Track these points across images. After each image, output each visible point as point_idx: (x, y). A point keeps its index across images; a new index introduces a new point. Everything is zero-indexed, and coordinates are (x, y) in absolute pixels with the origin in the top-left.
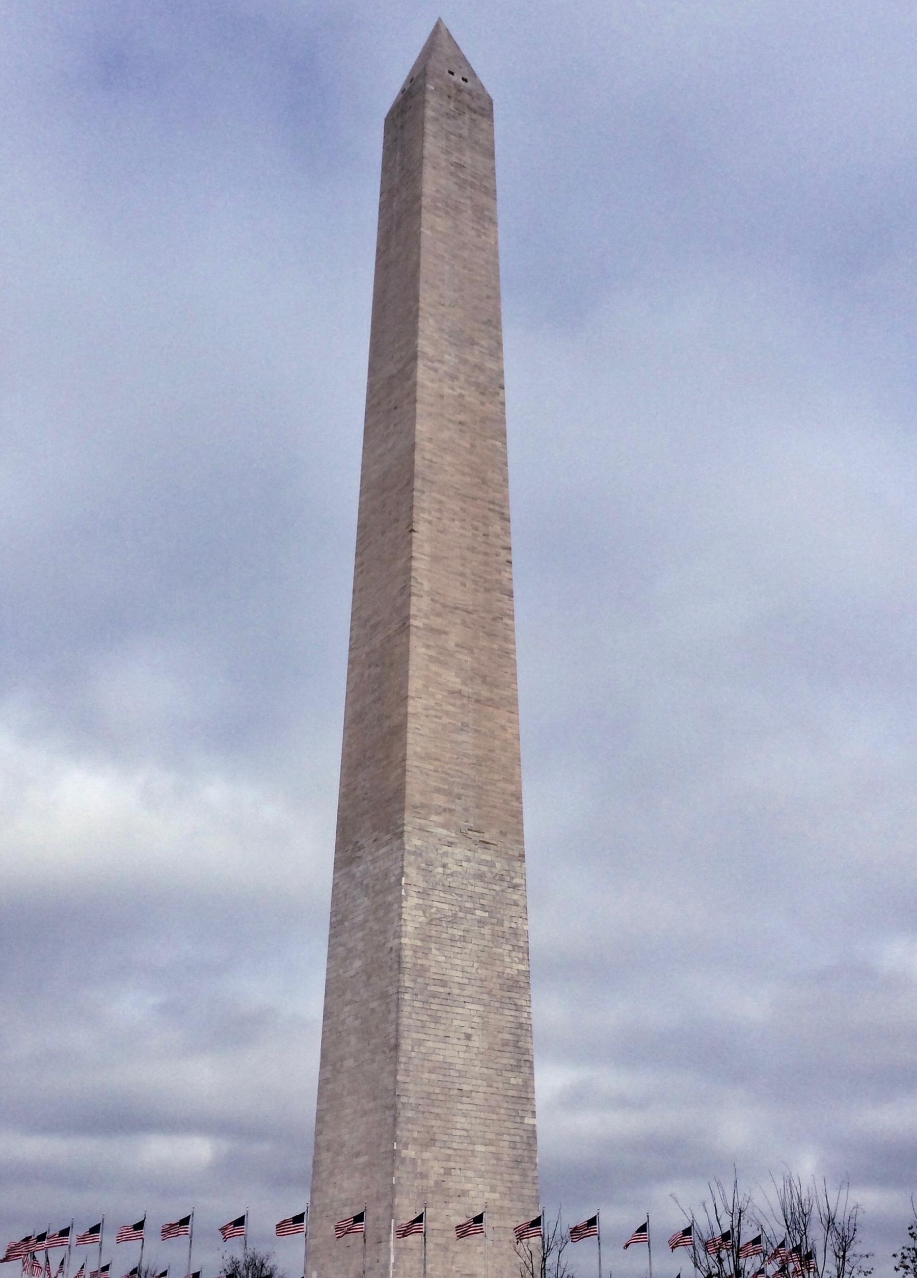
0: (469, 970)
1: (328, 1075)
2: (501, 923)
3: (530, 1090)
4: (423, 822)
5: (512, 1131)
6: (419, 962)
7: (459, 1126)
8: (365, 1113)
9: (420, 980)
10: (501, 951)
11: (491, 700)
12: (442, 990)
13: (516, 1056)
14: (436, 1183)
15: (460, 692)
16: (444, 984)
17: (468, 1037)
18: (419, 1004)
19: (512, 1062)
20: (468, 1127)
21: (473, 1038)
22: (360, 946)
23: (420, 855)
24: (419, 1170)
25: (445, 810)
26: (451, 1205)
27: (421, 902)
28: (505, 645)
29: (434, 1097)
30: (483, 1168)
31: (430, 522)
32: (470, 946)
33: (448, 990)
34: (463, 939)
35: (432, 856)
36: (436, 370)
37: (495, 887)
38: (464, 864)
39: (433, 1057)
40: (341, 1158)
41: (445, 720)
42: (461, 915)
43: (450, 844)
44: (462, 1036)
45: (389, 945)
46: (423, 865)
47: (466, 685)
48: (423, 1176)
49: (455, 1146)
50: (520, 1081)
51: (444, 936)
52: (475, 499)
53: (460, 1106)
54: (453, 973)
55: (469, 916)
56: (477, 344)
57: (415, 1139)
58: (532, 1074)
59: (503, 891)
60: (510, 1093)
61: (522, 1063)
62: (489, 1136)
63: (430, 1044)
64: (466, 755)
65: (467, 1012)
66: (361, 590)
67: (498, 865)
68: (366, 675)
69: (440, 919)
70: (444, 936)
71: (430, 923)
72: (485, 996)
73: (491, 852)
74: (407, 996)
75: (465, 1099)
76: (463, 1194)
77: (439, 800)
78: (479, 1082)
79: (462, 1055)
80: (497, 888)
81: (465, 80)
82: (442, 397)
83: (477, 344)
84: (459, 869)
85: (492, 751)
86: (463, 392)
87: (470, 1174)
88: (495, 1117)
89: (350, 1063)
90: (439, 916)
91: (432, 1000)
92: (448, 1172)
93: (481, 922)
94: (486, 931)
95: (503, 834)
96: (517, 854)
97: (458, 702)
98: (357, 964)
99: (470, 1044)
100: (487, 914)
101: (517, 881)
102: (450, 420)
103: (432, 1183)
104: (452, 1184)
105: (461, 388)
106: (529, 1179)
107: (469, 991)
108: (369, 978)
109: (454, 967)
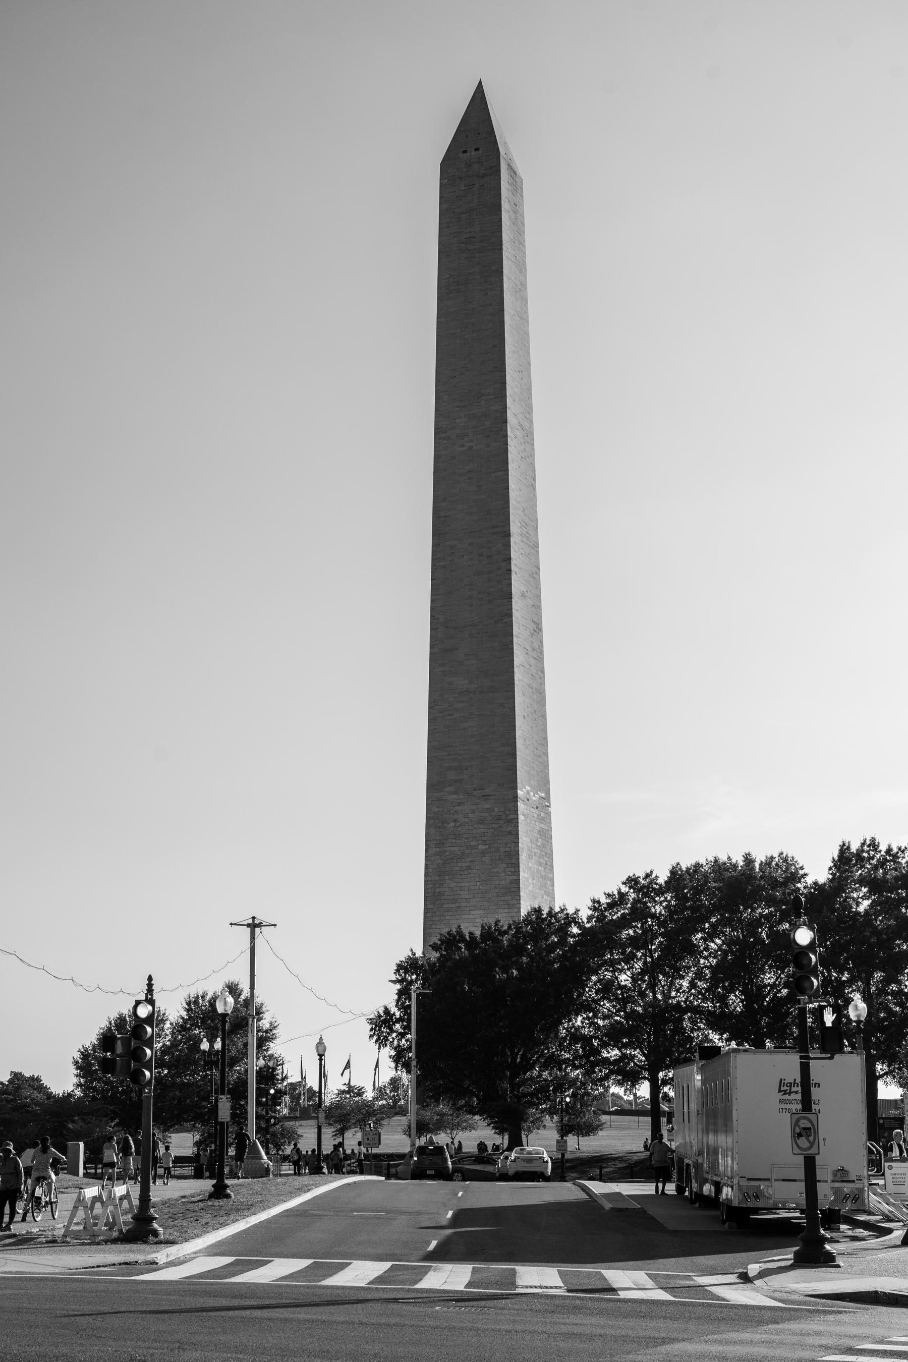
12: (453, 906)
16: (455, 901)
25: (456, 781)
27: (438, 850)
33: (457, 905)
34: (469, 868)
43: (459, 804)
55: (473, 851)
65: (471, 916)
67: (496, 810)
69: (452, 859)
80: (496, 826)
81: (477, 149)
82: (454, 458)
86: (471, 444)
93: (483, 853)
94: (487, 858)
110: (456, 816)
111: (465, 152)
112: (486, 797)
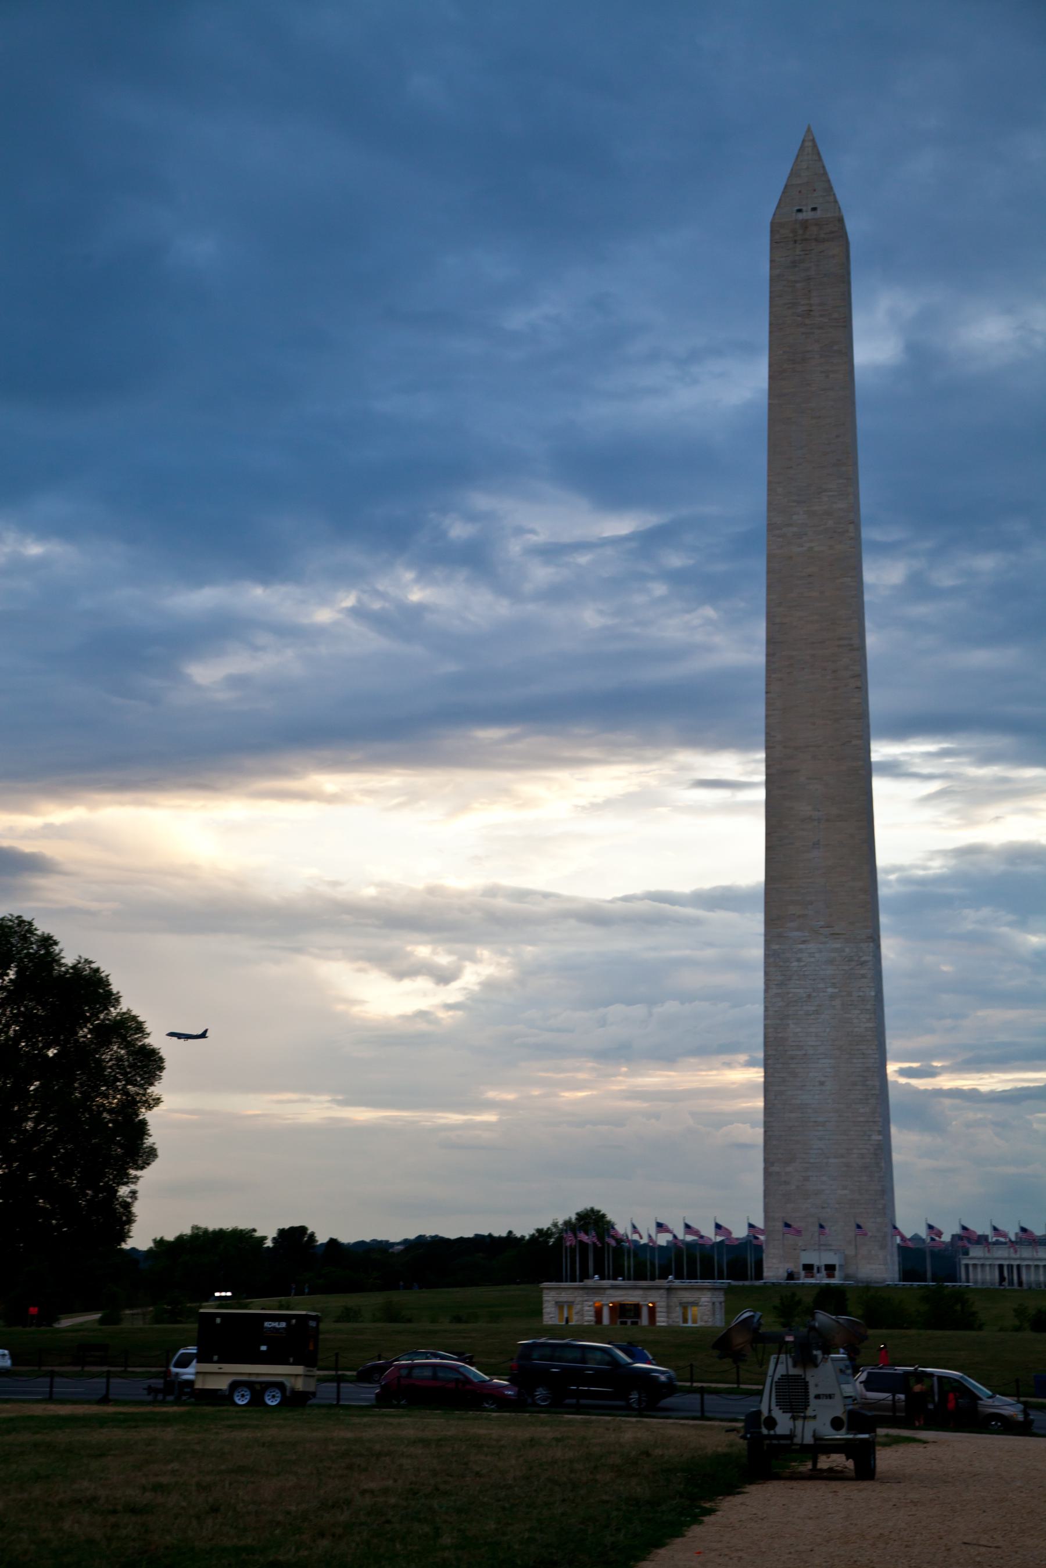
6: (780, 1035)
25: (799, 916)
27: (779, 991)
31: (781, 680)
33: (803, 1052)
38: (817, 955)
42: (814, 994)
43: (804, 942)
46: (781, 964)
48: (786, 1183)
49: (812, 1161)
55: (821, 994)
67: (847, 950)
74: (770, 1062)
75: (820, 1128)
79: (817, 1097)
80: (846, 968)
81: (814, 209)
87: (824, 1178)
93: (832, 997)
94: (837, 1002)
100: (836, 990)
111: (800, 211)
112: (835, 935)
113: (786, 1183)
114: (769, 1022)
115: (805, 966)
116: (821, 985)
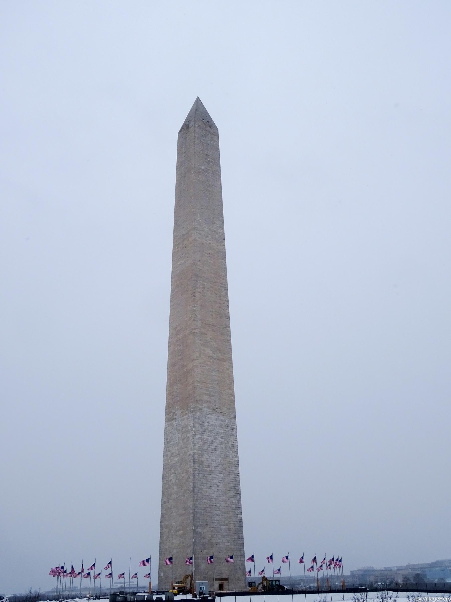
0: (218, 461)
1: (165, 500)
2: (228, 443)
3: (240, 504)
4: (199, 406)
5: (234, 520)
6: (200, 459)
7: (215, 519)
8: (181, 515)
9: (200, 466)
10: (228, 453)
11: (222, 359)
12: (208, 469)
13: (235, 492)
14: (209, 541)
15: (212, 357)
16: (209, 467)
17: (218, 486)
18: (201, 475)
19: (233, 494)
20: (218, 519)
21: (220, 486)
22: (177, 452)
23: (200, 419)
24: (202, 536)
25: (208, 402)
26: (214, 548)
27: (200, 436)
28: (227, 338)
29: (207, 509)
30: (224, 534)
31: (200, 293)
32: (218, 452)
35: (204, 419)
36: (200, 234)
37: (226, 429)
39: (206, 494)
40: (172, 532)
41: (207, 367)
43: (210, 414)
44: (216, 486)
45: (189, 453)
46: (201, 423)
47: (214, 354)
48: (204, 538)
49: (215, 526)
50: (236, 502)
51: (209, 449)
52: (215, 283)
53: (216, 512)
54: (212, 462)
55: (217, 441)
56: (215, 223)
57: (201, 525)
58: (240, 498)
59: (229, 431)
60: (233, 506)
61: (237, 495)
62: (226, 522)
63: (205, 490)
64: (215, 381)
65: (217, 477)
66: (173, 316)
68: (176, 348)
70: (209, 449)
71: (204, 444)
72: (224, 471)
73: (225, 416)
74: (196, 472)
75: (217, 509)
76: (217, 544)
77: (206, 398)
78: (222, 503)
82: (203, 244)
83: (215, 223)
84: (213, 423)
85: (224, 378)
87: (220, 536)
88: (228, 515)
89: (174, 496)
90: (207, 441)
91: (205, 473)
92: (212, 536)
93: (221, 443)
94: (223, 446)
95: (228, 409)
96: (233, 416)
97: (212, 361)
98: (176, 459)
99: (219, 489)
100: (223, 440)
101: (233, 427)
102: (206, 253)
103: (207, 541)
104: (213, 541)
105: (210, 240)
106: (240, 537)
107: (218, 468)
108: (181, 464)
109: (212, 460)
110: (208, 420)
113: (204, 538)
114: (196, 451)
115: (211, 426)
116: (217, 437)
